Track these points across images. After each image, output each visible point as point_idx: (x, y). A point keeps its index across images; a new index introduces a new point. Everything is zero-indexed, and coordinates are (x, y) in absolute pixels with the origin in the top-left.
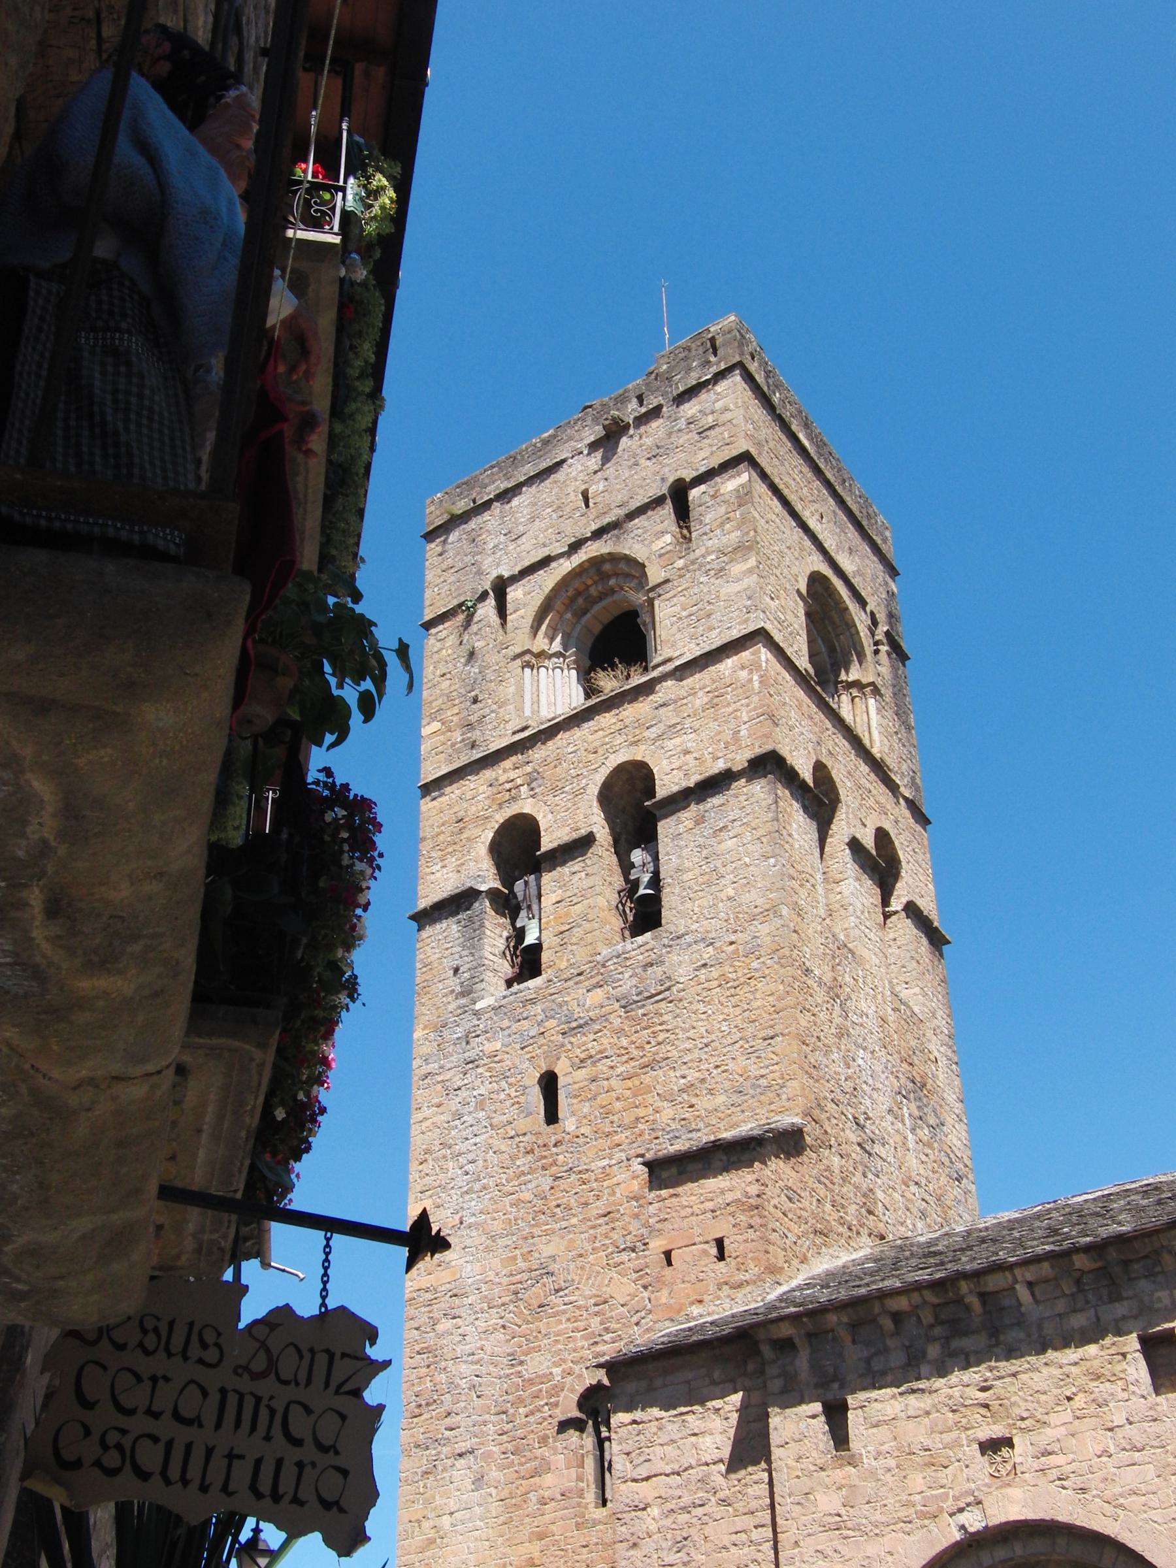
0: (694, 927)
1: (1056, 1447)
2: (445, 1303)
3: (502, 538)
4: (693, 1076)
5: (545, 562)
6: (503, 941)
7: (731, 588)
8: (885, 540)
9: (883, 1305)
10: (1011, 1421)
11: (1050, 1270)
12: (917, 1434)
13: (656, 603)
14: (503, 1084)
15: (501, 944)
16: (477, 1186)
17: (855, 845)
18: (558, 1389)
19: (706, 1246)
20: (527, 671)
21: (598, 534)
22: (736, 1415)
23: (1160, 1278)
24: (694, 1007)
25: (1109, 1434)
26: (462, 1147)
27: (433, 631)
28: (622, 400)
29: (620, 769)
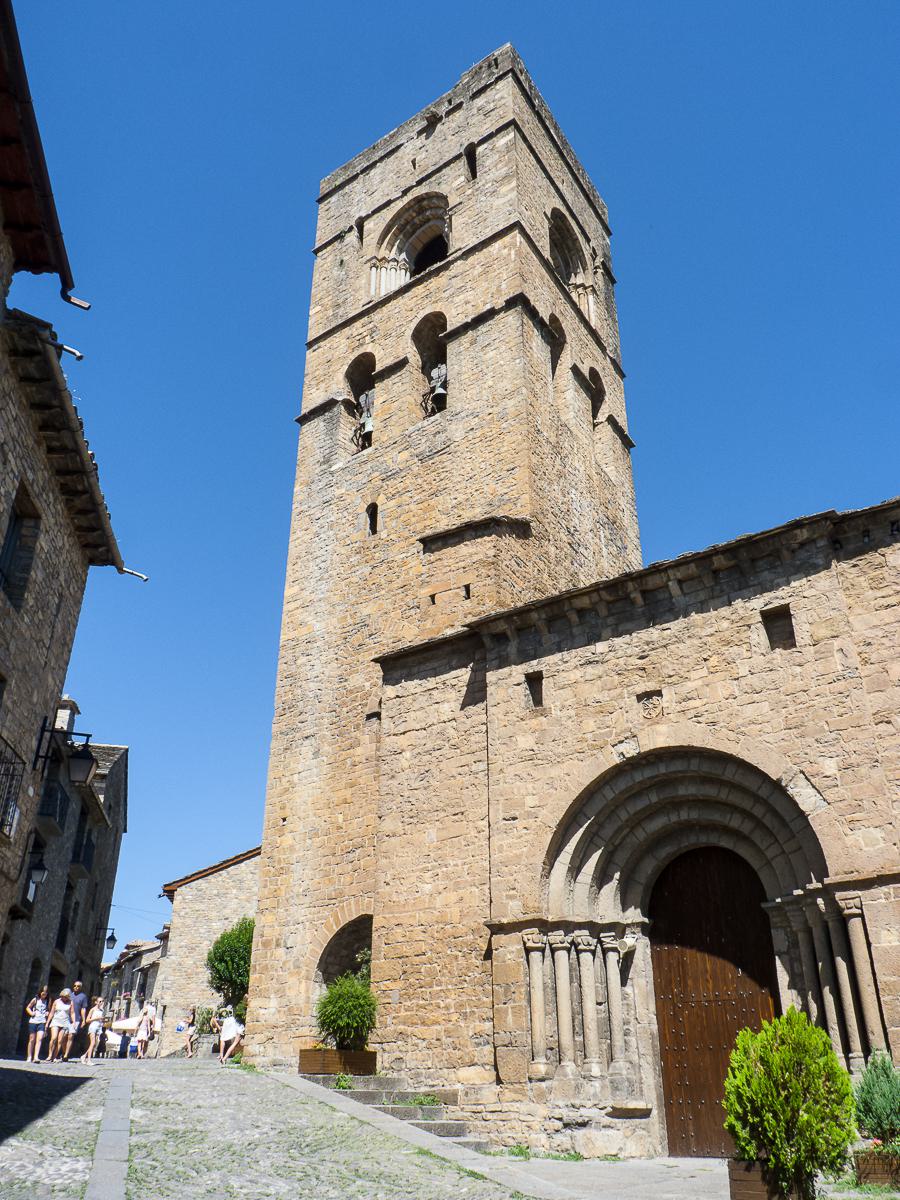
0: (466, 407)
1: (694, 694)
2: (303, 647)
3: (363, 195)
4: (461, 498)
5: (388, 203)
6: (352, 432)
7: (498, 202)
8: (604, 213)
9: (571, 603)
10: (661, 679)
11: (695, 569)
12: (592, 692)
13: (453, 218)
14: (345, 514)
15: (351, 434)
16: (326, 576)
17: (575, 370)
18: (367, 695)
19: (457, 590)
20: (374, 269)
21: (419, 183)
22: (466, 688)
23: (780, 570)
24: (463, 456)
25: (736, 682)
26: (319, 553)
27: (320, 254)
28: (438, 104)
29: (426, 319)
